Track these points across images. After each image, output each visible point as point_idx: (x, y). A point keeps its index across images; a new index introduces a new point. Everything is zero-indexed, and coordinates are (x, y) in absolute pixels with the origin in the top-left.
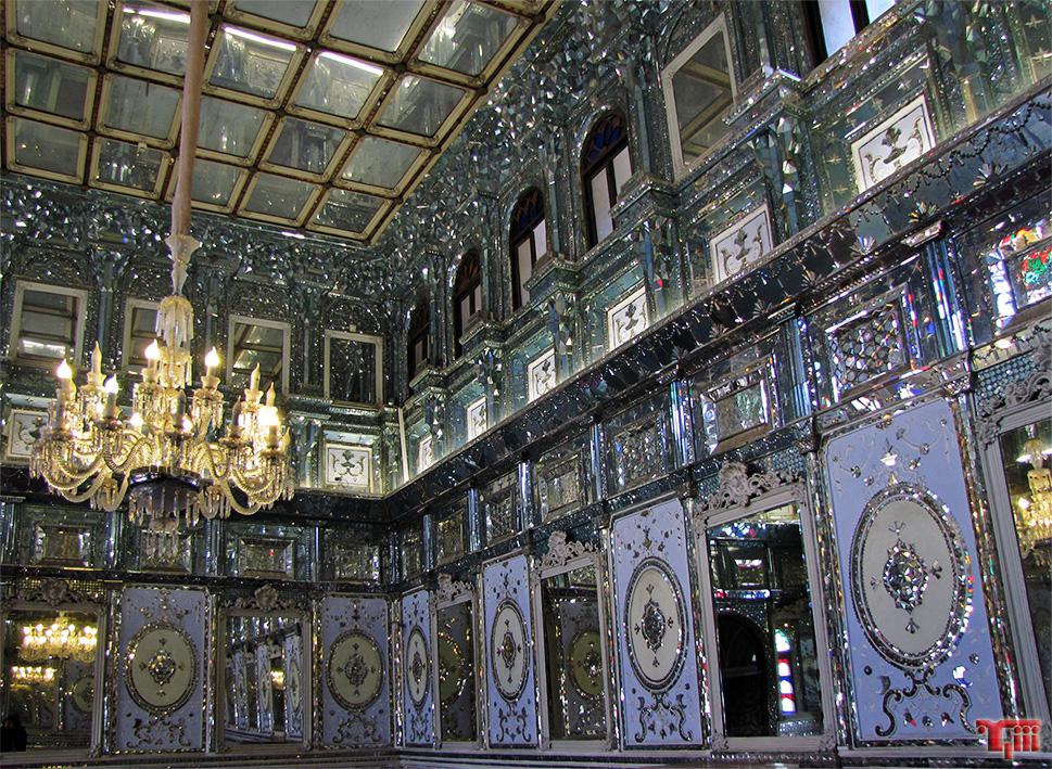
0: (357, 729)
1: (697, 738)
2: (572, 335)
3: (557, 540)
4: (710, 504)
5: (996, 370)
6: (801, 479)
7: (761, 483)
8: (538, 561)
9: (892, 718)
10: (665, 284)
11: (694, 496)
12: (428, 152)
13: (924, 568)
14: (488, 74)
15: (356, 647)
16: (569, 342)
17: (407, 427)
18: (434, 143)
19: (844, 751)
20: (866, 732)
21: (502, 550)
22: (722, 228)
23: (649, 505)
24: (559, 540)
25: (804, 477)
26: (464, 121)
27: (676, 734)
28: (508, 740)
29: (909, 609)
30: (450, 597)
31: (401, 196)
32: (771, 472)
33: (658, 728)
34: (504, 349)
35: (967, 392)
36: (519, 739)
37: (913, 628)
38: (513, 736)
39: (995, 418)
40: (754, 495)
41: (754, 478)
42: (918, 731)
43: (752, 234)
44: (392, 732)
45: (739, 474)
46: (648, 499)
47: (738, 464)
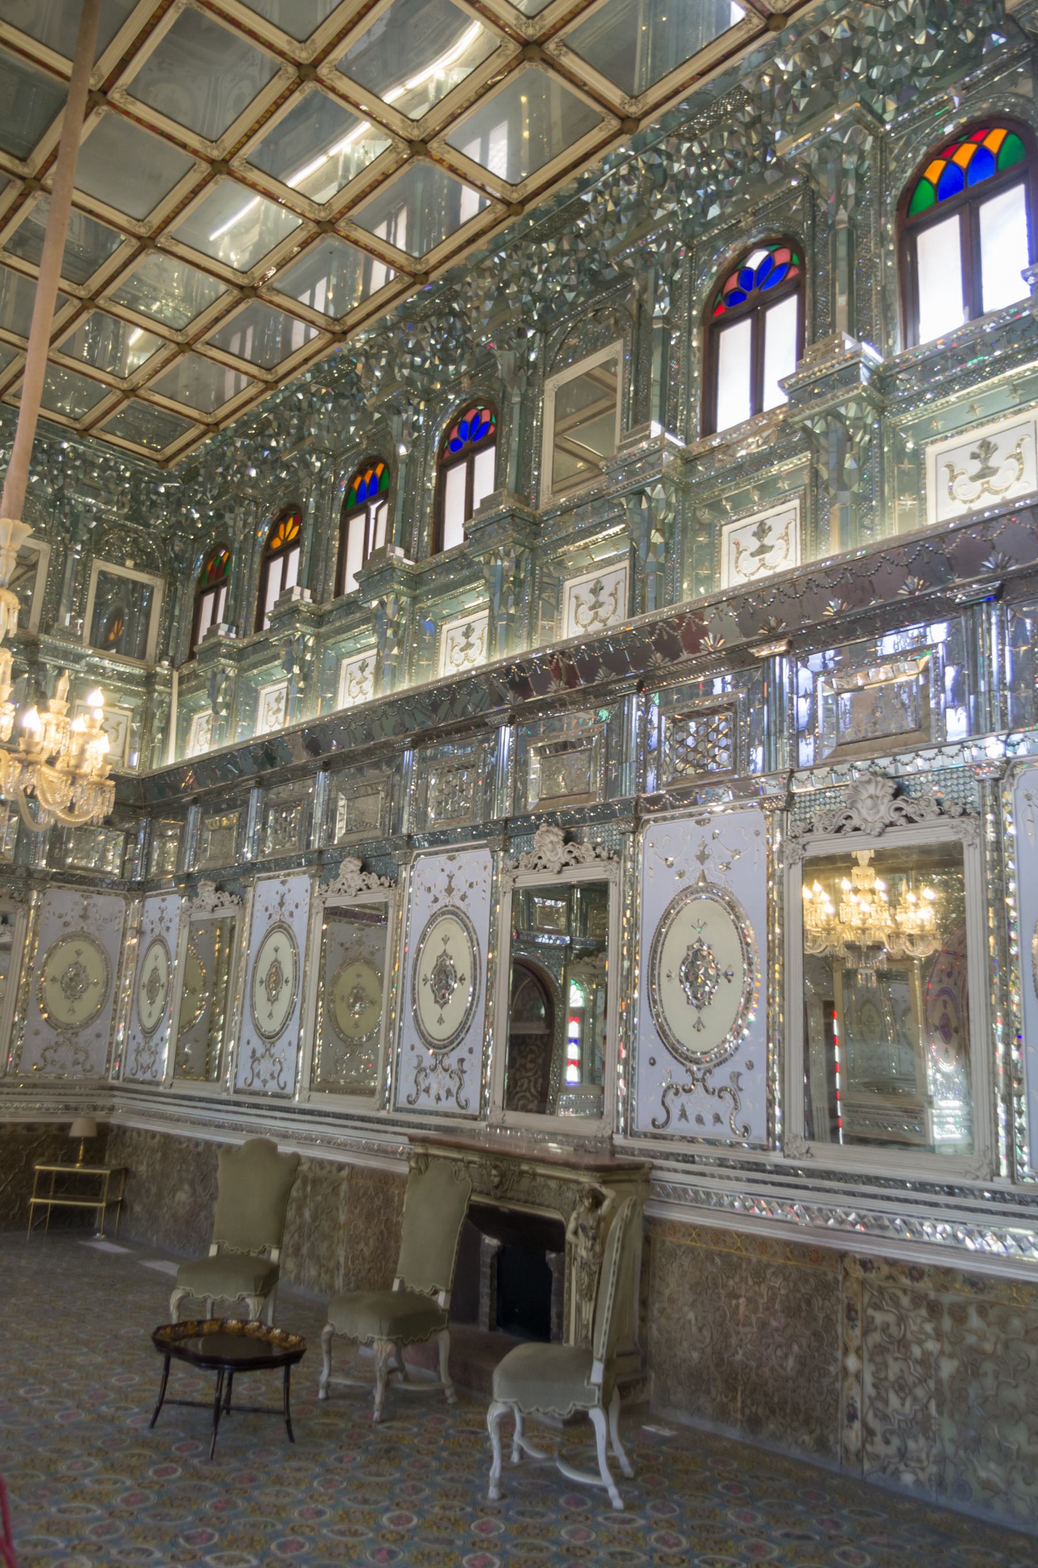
0: (65, 1054)
1: (474, 1108)
2: (400, 644)
3: (350, 866)
4: (522, 864)
5: (813, 798)
6: (616, 858)
7: (576, 853)
8: (324, 887)
9: (668, 1112)
10: (511, 618)
11: (506, 850)
12: (261, 386)
13: (717, 969)
14: (350, 320)
15: (78, 953)
16: (395, 651)
17: (180, 694)
18: (269, 377)
19: (619, 1140)
20: (643, 1123)
21: (281, 864)
22: (578, 572)
23: (457, 850)
24: (352, 867)
25: (619, 857)
26: (311, 363)
27: (452, 1100)
28: (257, 1085)
29: (698, 1007)
30: (209, 908)
31: (217, 424)
32: (587, 845)
33: (433, 1092)
34: (317, 637)
35: (782, 810)
36: (272, 1087)
37: (699, 1026)
38: (265, 1082)
39: (802, 841)
40: (567, 864)
41: (569, 847)
42: (689, 1128)
43: (609, 588)
44: (108, 1061)
45: (555, 839)
46: (456, 842)
47: (556, 830)
